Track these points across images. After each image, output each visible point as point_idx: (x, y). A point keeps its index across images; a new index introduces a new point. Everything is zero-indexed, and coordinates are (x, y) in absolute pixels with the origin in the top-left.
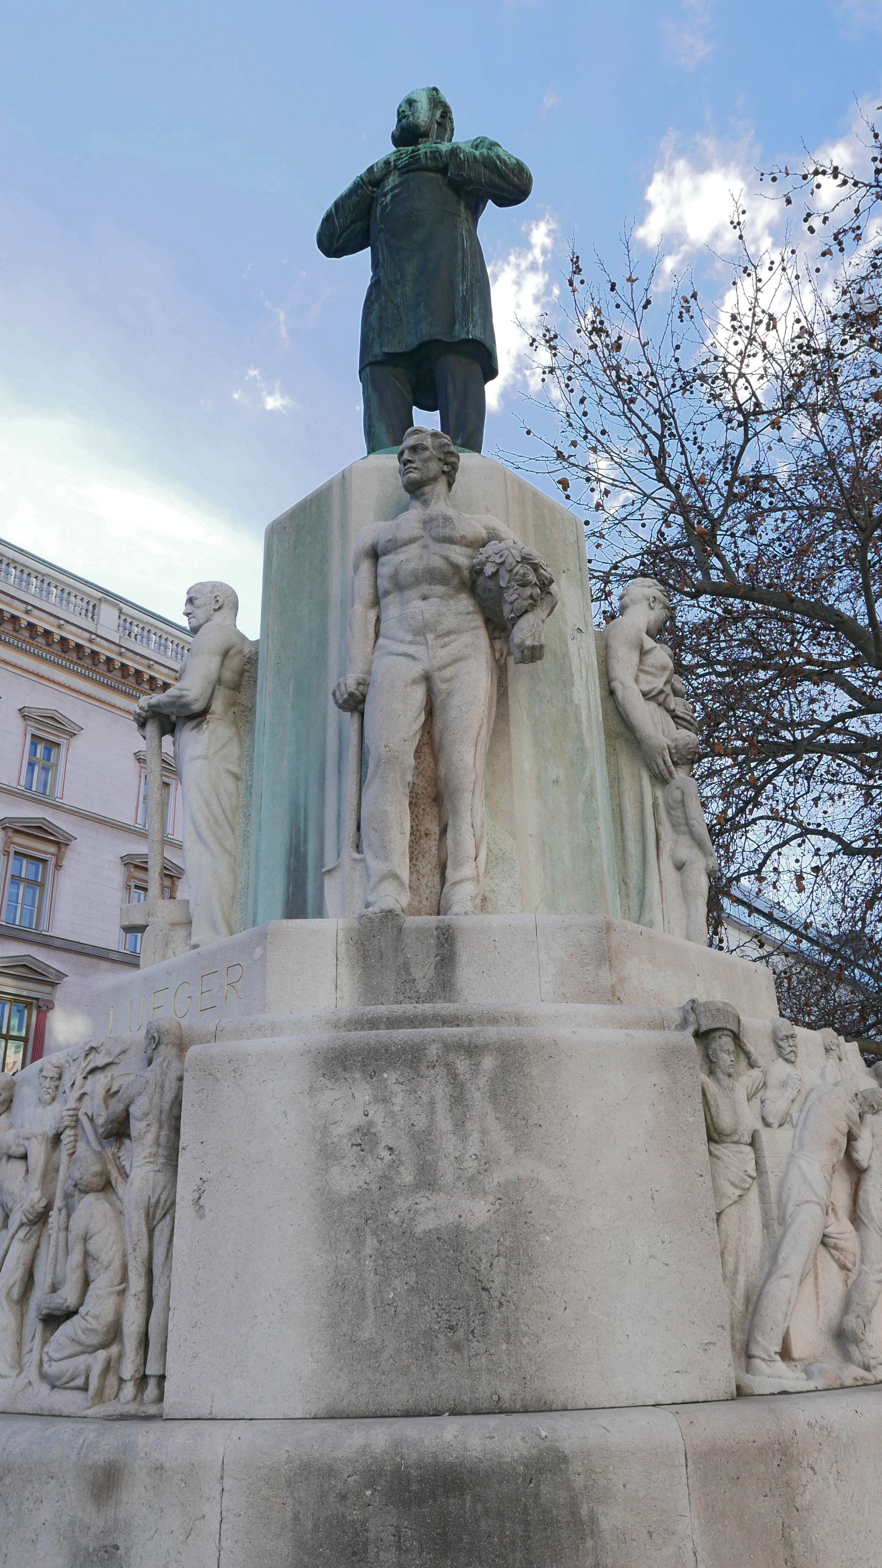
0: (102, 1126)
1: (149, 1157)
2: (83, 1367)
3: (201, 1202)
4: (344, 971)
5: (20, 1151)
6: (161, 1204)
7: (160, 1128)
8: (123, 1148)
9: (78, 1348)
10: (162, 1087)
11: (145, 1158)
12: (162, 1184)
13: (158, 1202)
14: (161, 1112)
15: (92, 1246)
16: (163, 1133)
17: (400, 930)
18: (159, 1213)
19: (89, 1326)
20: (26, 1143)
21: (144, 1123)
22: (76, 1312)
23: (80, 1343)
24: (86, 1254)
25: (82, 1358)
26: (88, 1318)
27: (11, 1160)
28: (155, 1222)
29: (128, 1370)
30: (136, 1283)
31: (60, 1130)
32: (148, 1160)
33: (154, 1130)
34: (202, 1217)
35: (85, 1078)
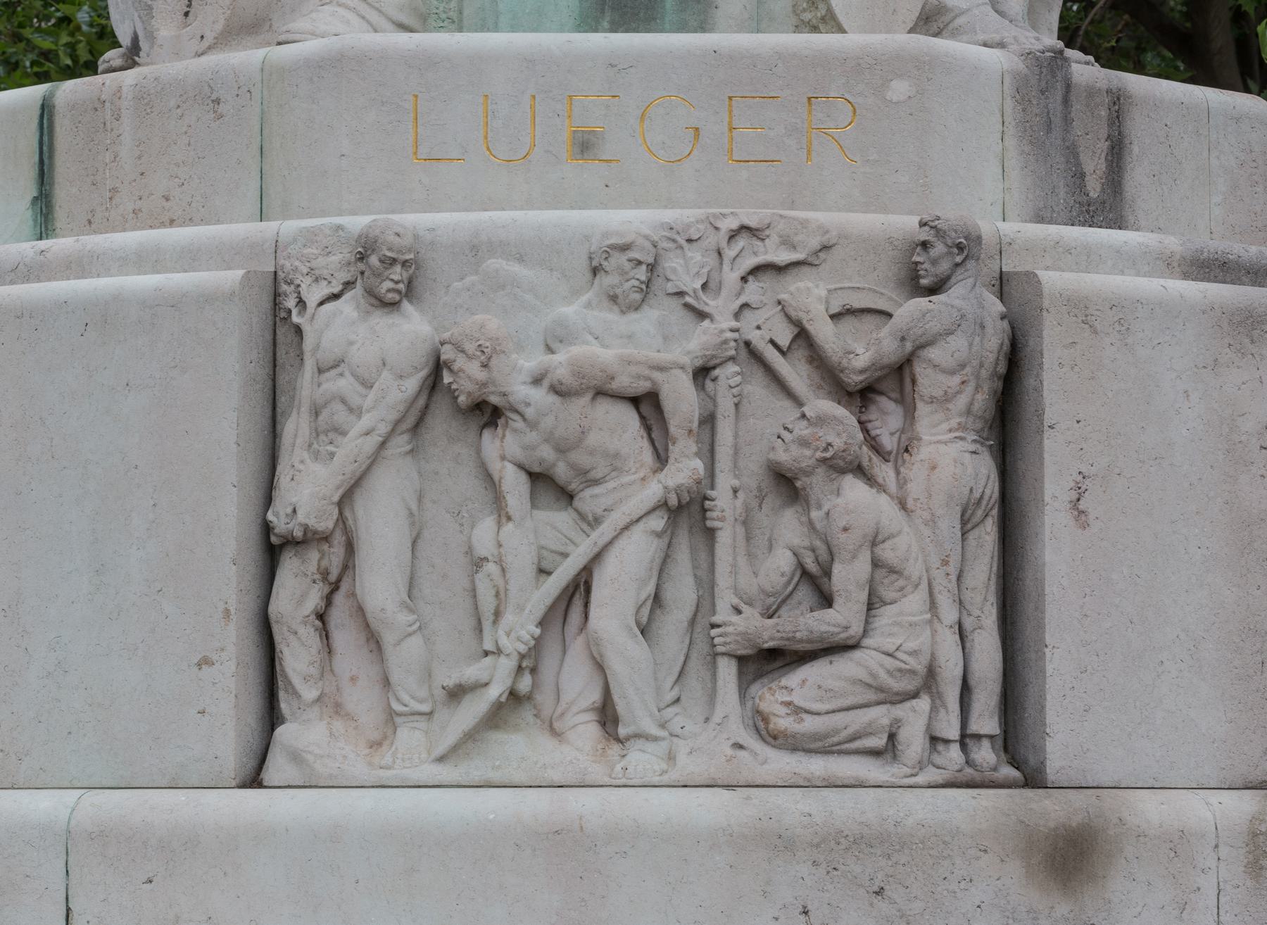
0: (862, 372)
1: (957, 430)
2: (886, 721)
3: (1082, 505)
4: (1011, 142)
5: (642, 387)
6: (984, 502)
7: (977, 388)
8: (873, 408)
9: (871, 696)
10: (983, 327)
11: (950, 431)
12: (984, 471)
13: (981, 497)
14: (981, 365)
15: (887, 553)
16: (979, 397)
17: (1068, 87)
18: (980, 513)
19: (903, 666)
20: (657, 375)
21: (956, 380)
22: (854, 646)
23: (880, 689)
24: (876, 564)
25: (882, 709)
26: (899, 654)
27: (600, 400)
28: (969, 526)
29: (951, 729)
30: (949, 614)
31: (711, 363)
32: (957, 434)
33: (970, 389)
34: (1085, 526)
35: (744, 279)
